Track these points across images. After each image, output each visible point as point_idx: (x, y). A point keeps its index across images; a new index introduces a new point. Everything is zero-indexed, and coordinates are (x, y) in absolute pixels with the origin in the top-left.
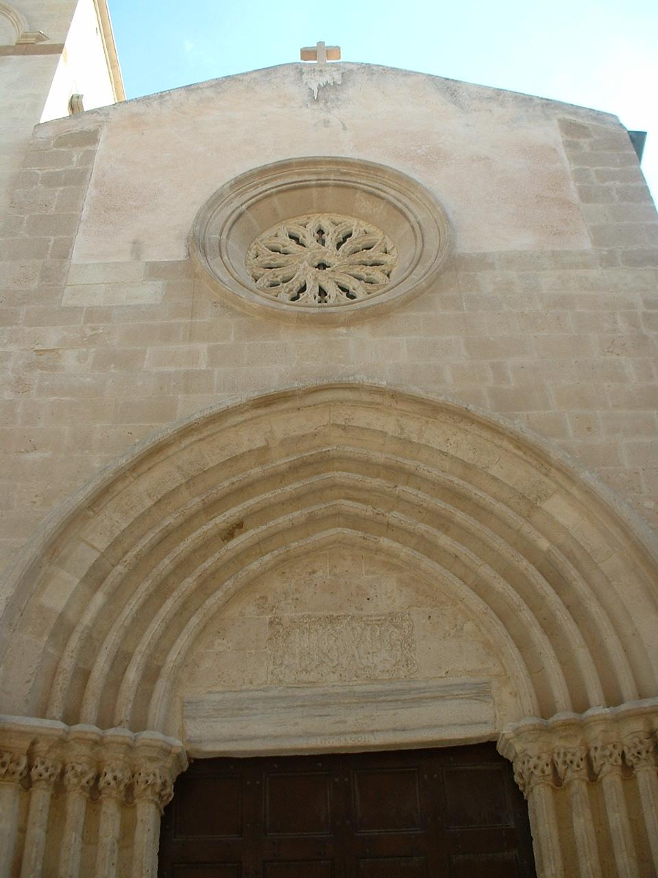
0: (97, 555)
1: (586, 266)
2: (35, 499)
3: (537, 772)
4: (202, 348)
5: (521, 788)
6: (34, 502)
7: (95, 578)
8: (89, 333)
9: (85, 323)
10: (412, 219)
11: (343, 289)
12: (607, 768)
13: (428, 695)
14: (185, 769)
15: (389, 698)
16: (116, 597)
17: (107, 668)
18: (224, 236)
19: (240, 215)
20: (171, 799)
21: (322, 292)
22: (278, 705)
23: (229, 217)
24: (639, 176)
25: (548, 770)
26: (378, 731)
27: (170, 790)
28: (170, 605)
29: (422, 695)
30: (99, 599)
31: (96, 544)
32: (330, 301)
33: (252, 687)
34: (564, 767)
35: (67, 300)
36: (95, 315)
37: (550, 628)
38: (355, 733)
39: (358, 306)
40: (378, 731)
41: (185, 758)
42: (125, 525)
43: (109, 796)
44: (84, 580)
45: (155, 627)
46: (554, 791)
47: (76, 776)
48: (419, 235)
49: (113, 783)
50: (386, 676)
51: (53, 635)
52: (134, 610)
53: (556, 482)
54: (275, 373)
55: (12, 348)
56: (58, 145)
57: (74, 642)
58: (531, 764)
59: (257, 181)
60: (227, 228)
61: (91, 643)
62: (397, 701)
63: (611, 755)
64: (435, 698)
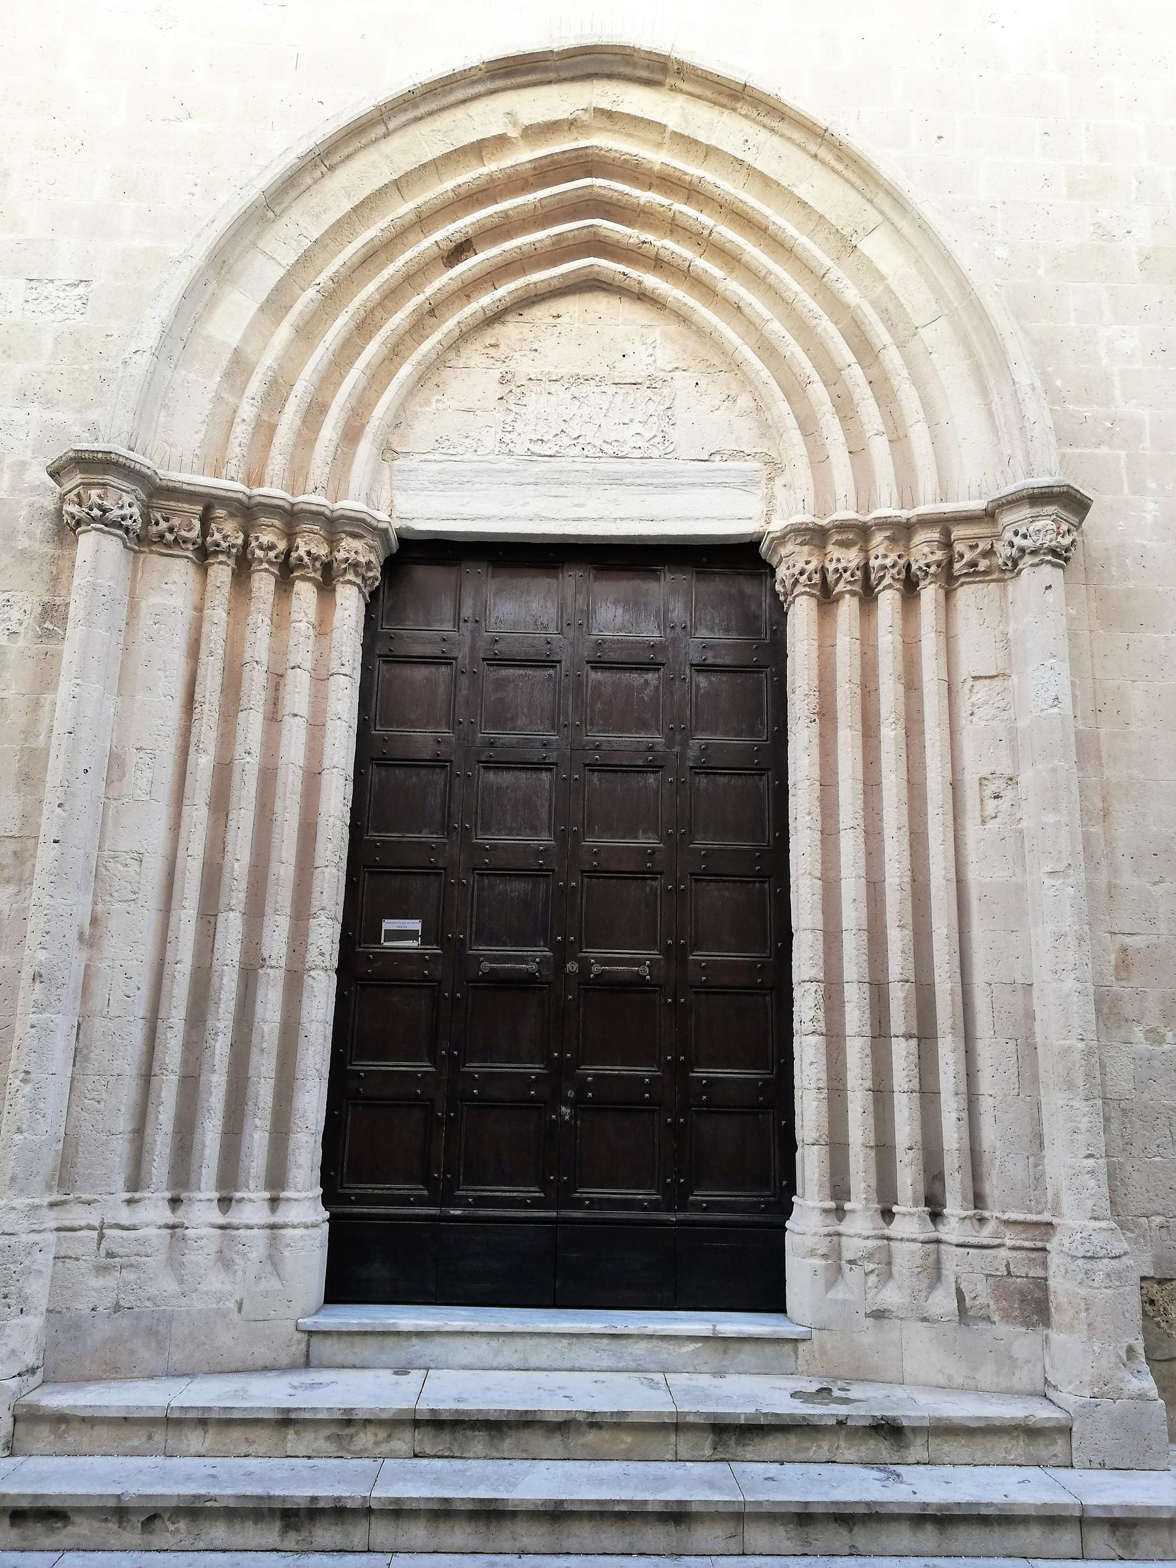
0: (281, 272)
2: (195, 190)
3: (803, 579)
5: (782, 598)
6: (193, 195)
7: (276, 303)
13: (685, 480)
14: (395, 551)
15: (638, 481)
16: (307, 332)
17: (298, 422)
20: (377, 584)
22: (507, 480)
25: (817, 578)
26: (622, 519)
27: (376, 573)
28: (372, 350)
29: (678, 480)
30: (284, 332)
31: (279, 259)
33: (476, 458)
34: (836, 576)
37: (845, 408)
38: (595, 520)
40: (622, 519)
41: (393, 537)
42: (316, 235)
43: (304, 578)
44: (262, 309)
46: (820, 604)
47: (261, 547)
49: (306, 559)
50: (638, 454)
51: (228, 375)
52: (331, 349)
53: (882, 213)
57: (256, 385)
58: (796, 571)
61: (276, 392)
62: (647, 485)
63: (893, 566)
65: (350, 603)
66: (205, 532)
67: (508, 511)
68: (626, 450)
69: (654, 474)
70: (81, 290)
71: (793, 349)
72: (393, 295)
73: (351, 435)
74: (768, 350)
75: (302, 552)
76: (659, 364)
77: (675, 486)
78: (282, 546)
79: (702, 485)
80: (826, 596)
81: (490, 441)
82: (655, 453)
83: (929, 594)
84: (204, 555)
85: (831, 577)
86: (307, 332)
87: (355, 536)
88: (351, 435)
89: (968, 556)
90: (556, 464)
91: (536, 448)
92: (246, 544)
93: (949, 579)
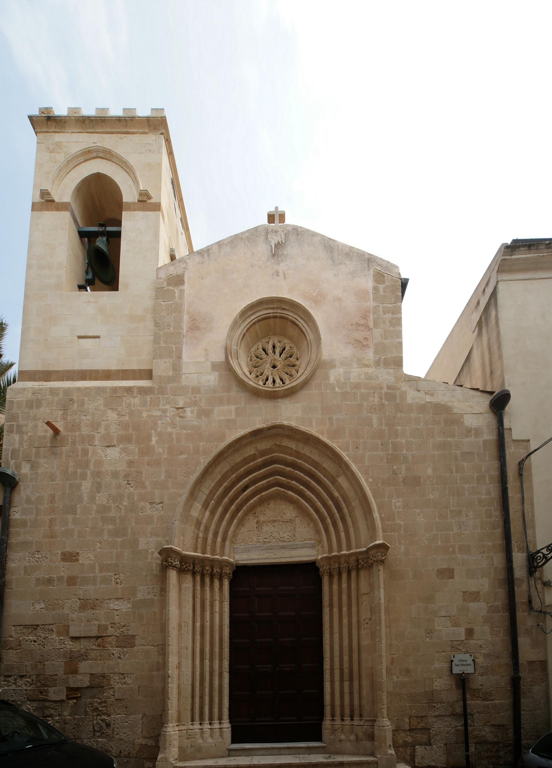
1: (367, 366)
4: (233, 407)
8: (194, 399)
9: (192, 394)
10: (308, 338)
11: (282, 380)
12: (344, 571)
16: (213, 513)
18: (238, 348)
19: (244, 335)
21: (274, 382)
23: (240, 336)
24: (398, 310)
27: (231, 575)
28: (228, 516)
32: (277, 385)
35: (184, 382)
36: (196, 390)
39: (286, 387)
45: (224, 523)
48: (309, 345)
51: (195, 526)
54: (259, 422)
55: (167, 407)
56: (169, 284)
59: (250, 313)
60: (239, 343)
61: (207, 529)
64: (301, 548)
65: (226, 583)
66: (194, 568)
67: (260, 557)
68: (285, 539)
69: (292, 545)
70: (162, 505)
71: (323, 510)
72: (232, 501)
73: (224, 540)
74: (317, 511)
75: (215, 571)
76: (293, 515)
77: (297, 548)
78: (210, 570)
79: (303, 548)
80: (331, 576)
81: (255, 539)
82: (292, 540)
83: (354, 574)
84: (194, 574)
85: (332, 570)
86: (213, 513)
87: (227, 566)
88: (224, 540)
89: (362, 563)
90: (270, 544)
91: (265, 540)
92: (203, 570)
93: (358, 570)
